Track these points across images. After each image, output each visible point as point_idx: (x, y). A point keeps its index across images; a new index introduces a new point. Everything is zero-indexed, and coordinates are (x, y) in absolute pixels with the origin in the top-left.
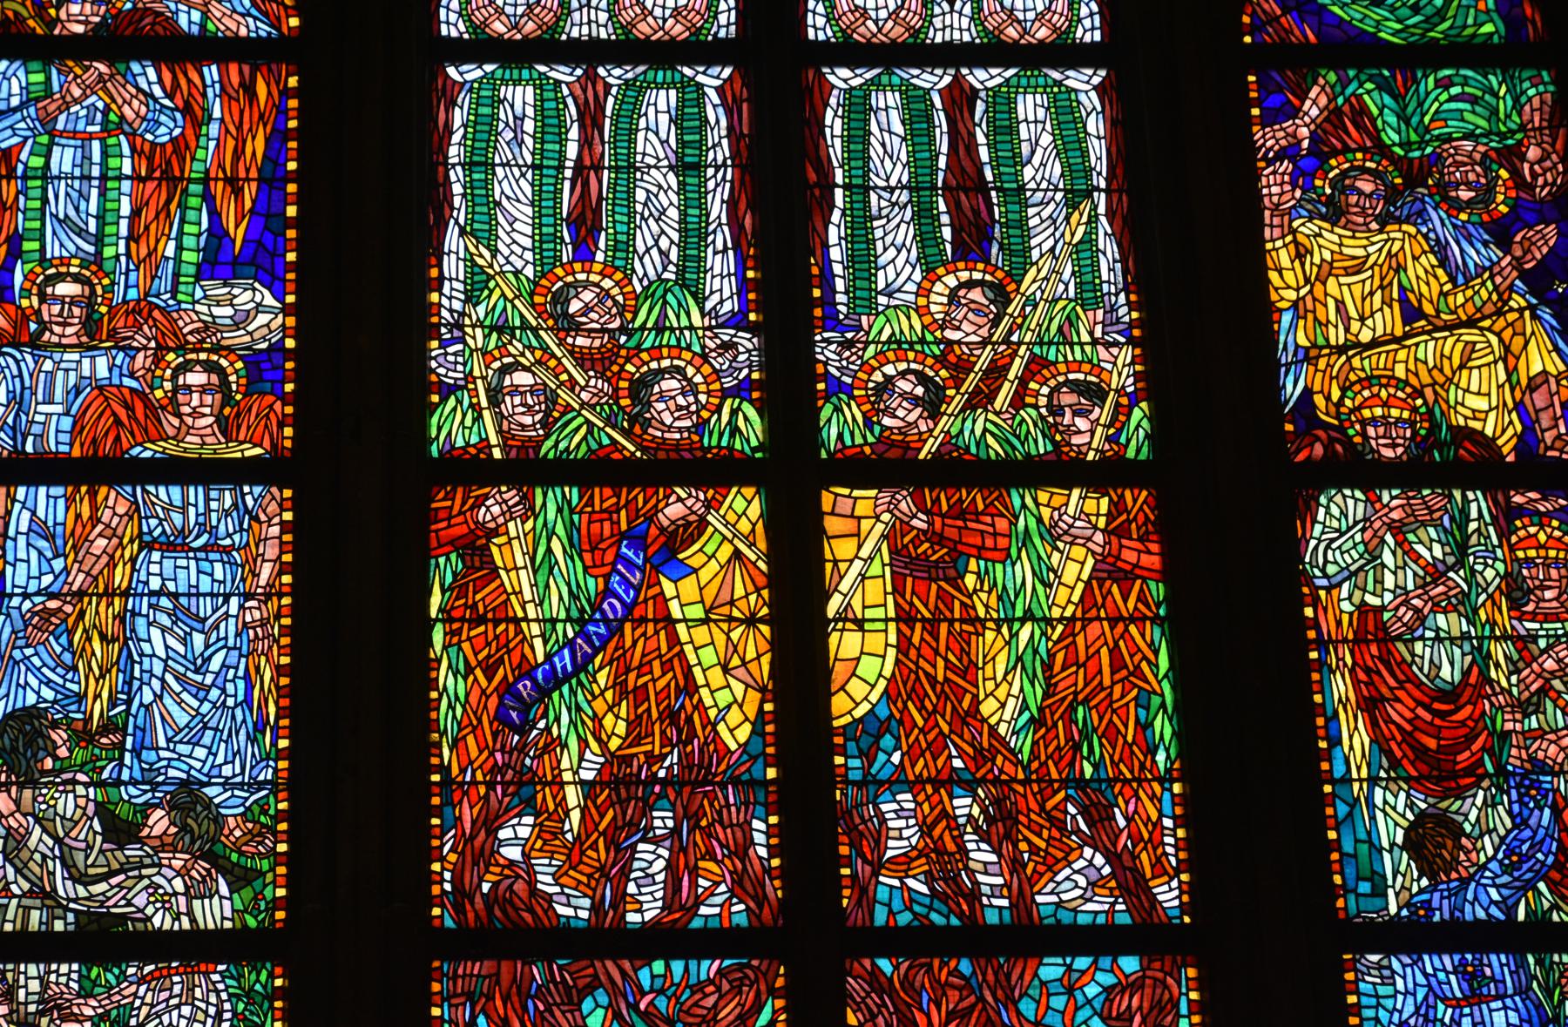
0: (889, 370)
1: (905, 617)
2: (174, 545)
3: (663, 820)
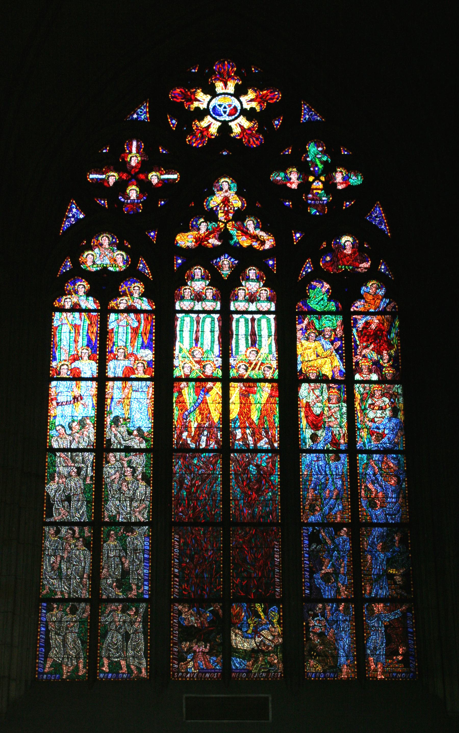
0: (241, 364)
1: (241, 403)
3: (205, 433)
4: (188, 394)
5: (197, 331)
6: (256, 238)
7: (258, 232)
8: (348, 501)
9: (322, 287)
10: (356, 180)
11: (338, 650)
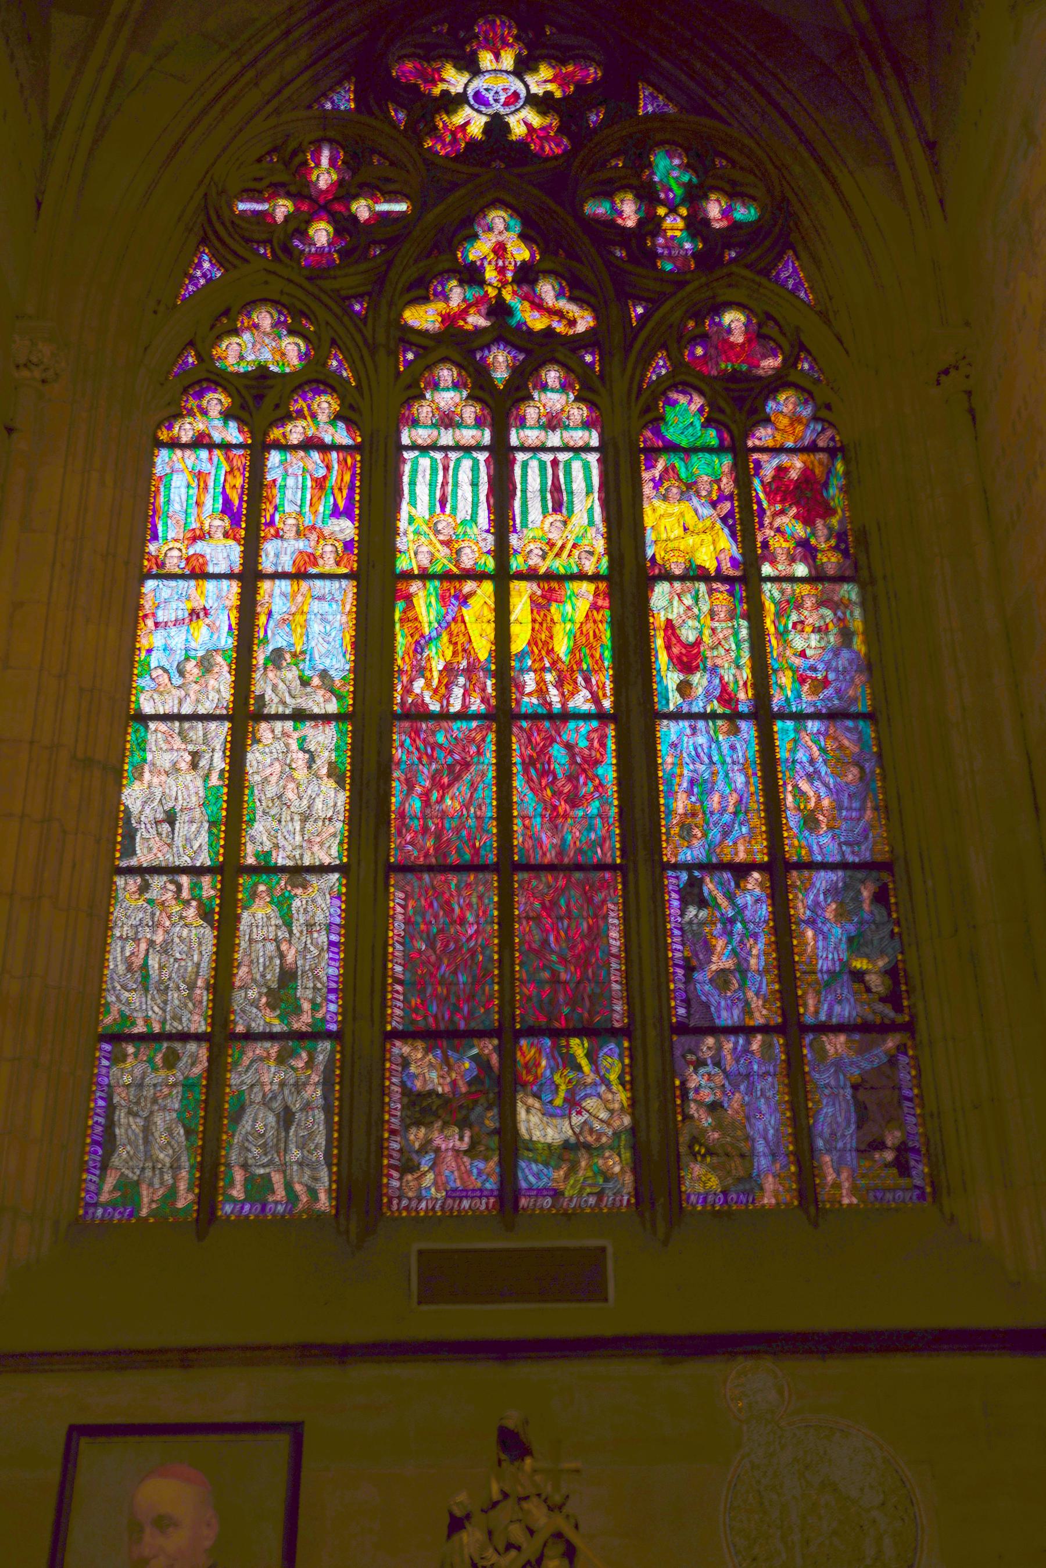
0: (532, 546)
1: (534, 621)
2: (321, 598)
3: (462, 680)
4: (426, 604)
5: (444, 484)
6: (560, 314)
7: (563, 304)
8: (760, 818)
9: (690, 402)
10: (744, 213)
11: (753, 1140)
